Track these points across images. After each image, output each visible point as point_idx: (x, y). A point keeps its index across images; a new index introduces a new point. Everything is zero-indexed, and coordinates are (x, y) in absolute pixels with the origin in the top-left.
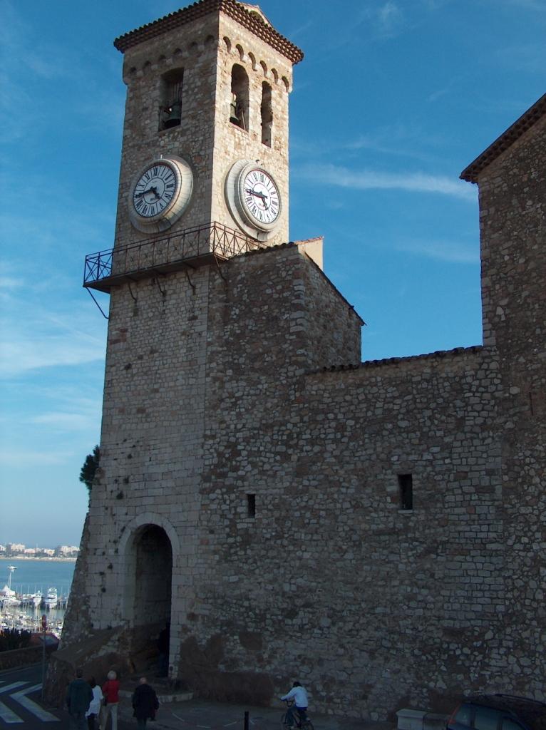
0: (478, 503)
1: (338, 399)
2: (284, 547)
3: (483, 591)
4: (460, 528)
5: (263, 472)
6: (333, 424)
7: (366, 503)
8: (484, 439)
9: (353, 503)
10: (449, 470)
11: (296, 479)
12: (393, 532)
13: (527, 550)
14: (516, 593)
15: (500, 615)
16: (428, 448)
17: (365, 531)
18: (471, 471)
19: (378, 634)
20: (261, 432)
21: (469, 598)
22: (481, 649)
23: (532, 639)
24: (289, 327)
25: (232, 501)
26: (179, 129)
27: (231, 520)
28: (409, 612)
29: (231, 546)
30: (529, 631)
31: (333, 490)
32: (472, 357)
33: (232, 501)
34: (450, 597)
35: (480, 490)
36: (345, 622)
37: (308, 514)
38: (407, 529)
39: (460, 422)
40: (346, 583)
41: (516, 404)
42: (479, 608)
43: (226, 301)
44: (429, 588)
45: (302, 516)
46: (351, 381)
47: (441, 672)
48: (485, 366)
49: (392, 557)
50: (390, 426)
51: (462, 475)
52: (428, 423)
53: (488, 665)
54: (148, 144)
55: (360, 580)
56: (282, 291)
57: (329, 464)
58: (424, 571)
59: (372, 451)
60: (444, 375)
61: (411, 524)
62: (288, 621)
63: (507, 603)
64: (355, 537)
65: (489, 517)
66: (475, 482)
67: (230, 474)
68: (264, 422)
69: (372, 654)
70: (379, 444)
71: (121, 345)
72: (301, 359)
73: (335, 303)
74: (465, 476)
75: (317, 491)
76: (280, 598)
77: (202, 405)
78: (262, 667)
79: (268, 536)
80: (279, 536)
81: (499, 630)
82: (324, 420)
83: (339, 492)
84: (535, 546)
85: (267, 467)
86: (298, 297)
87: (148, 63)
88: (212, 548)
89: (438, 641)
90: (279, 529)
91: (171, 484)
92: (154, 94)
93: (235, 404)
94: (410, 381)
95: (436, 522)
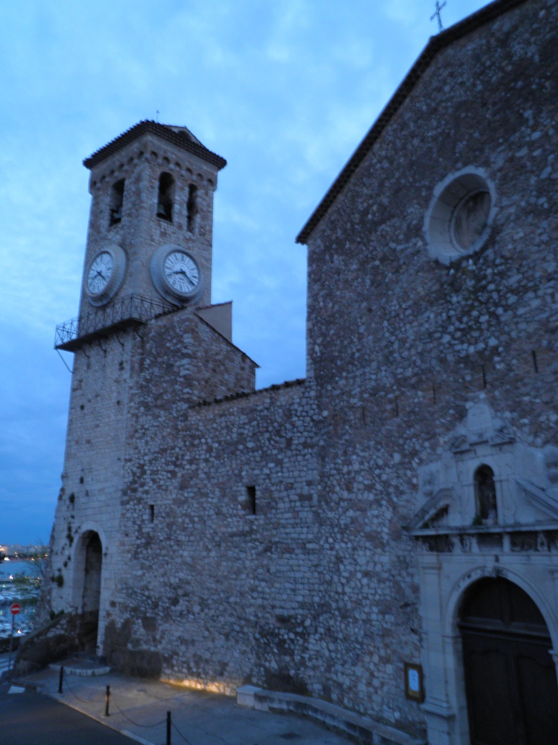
0: (301, 509)
1: (209, 427)
2: (171, 546)
3: (303, 584)
4: (287, 531)
5: (159, 487)
6: (205, 447)
7: (224, 510)
8: (304, 455)
9: (216, 510)
10: (281, 482)
11: (180, 492)
12: (243, 534)
13: (332, 549)
15: (316, 605)
16: (267, 464)
17: (224, 533)
18: (296, 482)
19: (232, 620)
20: (159, 455)
21: (294, 590)
22: (302, 635)
24: (179, 372)
25: (140, 510)
26: (119, 225)
27: (139, 526)
28: (252, 601)
29: (138, 547)
31: (204, 500)
32: (298, 387)
33: (140, 510)
34: (280, 589)
35: (303, 498)
36: (209, 609)
37: (187, 520)
38: (252, 531)
39: (289, 442)
40: (211, 576)
42: (300, 599)
43: (142, 354)
44: (266, 581)
45: (183, 523)
46: (217, 412)
47: (274, 653)
48: (307, 395)
49: (242, 555)
50: (241, 447)
51: (290, 486)
52: (267, 443)
53: (307, 649)
54: (101, 239)
55: (220, 573)
56: (176, 344)
57: (202, 480)
58: (263, 566)
59: (228, 468)
60: (278, 404)
61: (255, 527)
62: (173, 608)
64: (217, 539)
65: (309, 521)
66: (299, 491)
67: (140, 489)
68: (161, 447)
69: (227, 636)
70: (234, 462)
71: (79, 392)
72: (186, 396)
73: (227, 351)
74: (290, 487)
75: (193, 501)
76: (168, 588)
77: (124, 436)
78: (156, 646)
79: (161, 538)
80: (169, 538)
81: (315, 618)
82: (199, 444)
83: (207, 502)
84: (337, 546)
85: (162, 483)
86: (186, 347)
87: (104, 177)
88: (127, 548)
89: (272, 626)
90: (168, 532)
91: (103, 498)
92: (107, 201)
93: (144, 434)
94: (256, 410)
95: (271, 526)
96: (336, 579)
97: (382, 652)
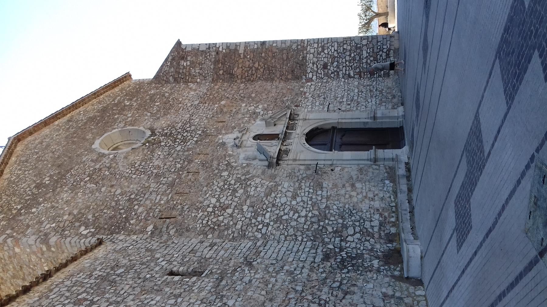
14: (299, 233)
23: (333, 226)
30: (327, 227)
41: (160, 227)
63: (305, 240)
96: (294, 223)
97: (349, 189)
